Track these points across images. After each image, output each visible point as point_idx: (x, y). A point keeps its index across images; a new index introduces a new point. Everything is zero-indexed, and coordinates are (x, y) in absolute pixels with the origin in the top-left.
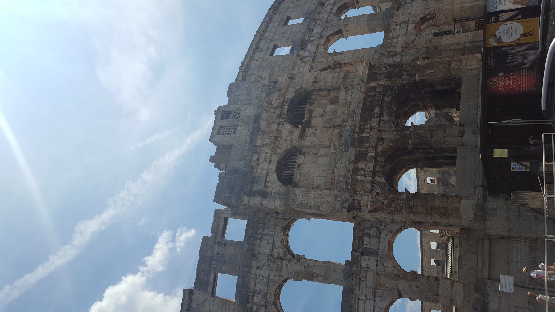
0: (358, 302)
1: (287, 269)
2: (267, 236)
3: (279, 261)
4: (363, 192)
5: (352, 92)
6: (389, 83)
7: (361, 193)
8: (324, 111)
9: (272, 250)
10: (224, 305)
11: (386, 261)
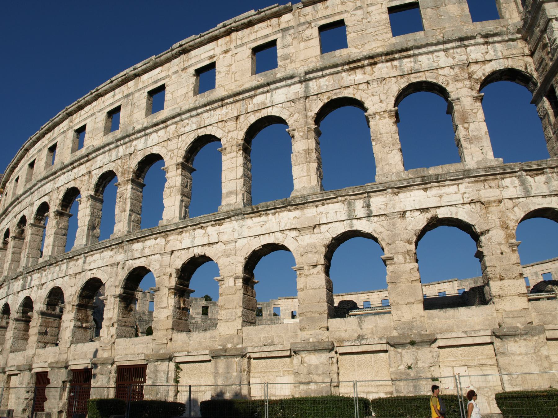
0: (454, 184)
1: (460, 89)
2: (493, 50)
3: (467, 76)
9: (477, 62)
10: (384, 27)
11: (521, 209)
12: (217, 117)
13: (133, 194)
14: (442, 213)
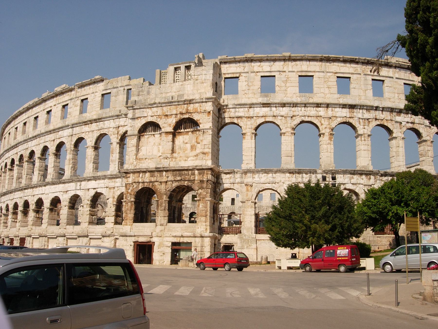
3: (117, 133)
4: (134, 178)
5: (193, 160)
6: (196, 182)
7: (134, 178)
8: (187, 143)
13: (28, 167)
14: (99, 191)
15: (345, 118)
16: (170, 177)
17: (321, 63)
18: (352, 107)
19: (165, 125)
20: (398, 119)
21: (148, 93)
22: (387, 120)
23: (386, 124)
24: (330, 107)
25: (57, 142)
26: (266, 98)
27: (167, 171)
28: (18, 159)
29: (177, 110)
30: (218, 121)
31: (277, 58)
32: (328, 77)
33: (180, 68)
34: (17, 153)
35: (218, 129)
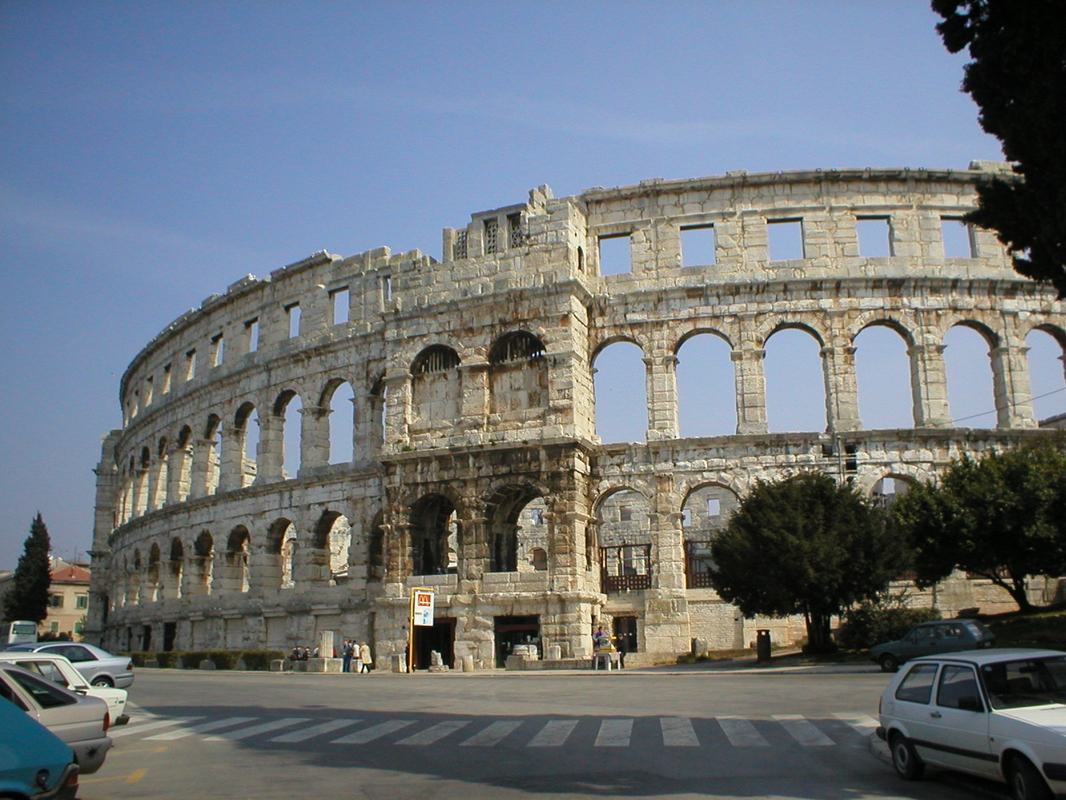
3: (365, 374)
5: (535, 427)
9: (375, 360)
12: (219, 398)
14: (331, 507)
15: (881, 311)
16: (483, 469)
17: (817, 189)
18: (896, 286)
19: (470, 351)
20: (1010, 304)
21: (429, 284)
22: (982, 310)
23: (980, 319)
24: (844, 288)
25: (238, 404)
26: (694, 278)
27: (476, 456)
28: (156, 449)
29: (493, 316)
30: (589, 335)
31: (714, 184)
32: (835, 219)
33: (495, 220)
34: (153, 435)
35: (588, 353)
